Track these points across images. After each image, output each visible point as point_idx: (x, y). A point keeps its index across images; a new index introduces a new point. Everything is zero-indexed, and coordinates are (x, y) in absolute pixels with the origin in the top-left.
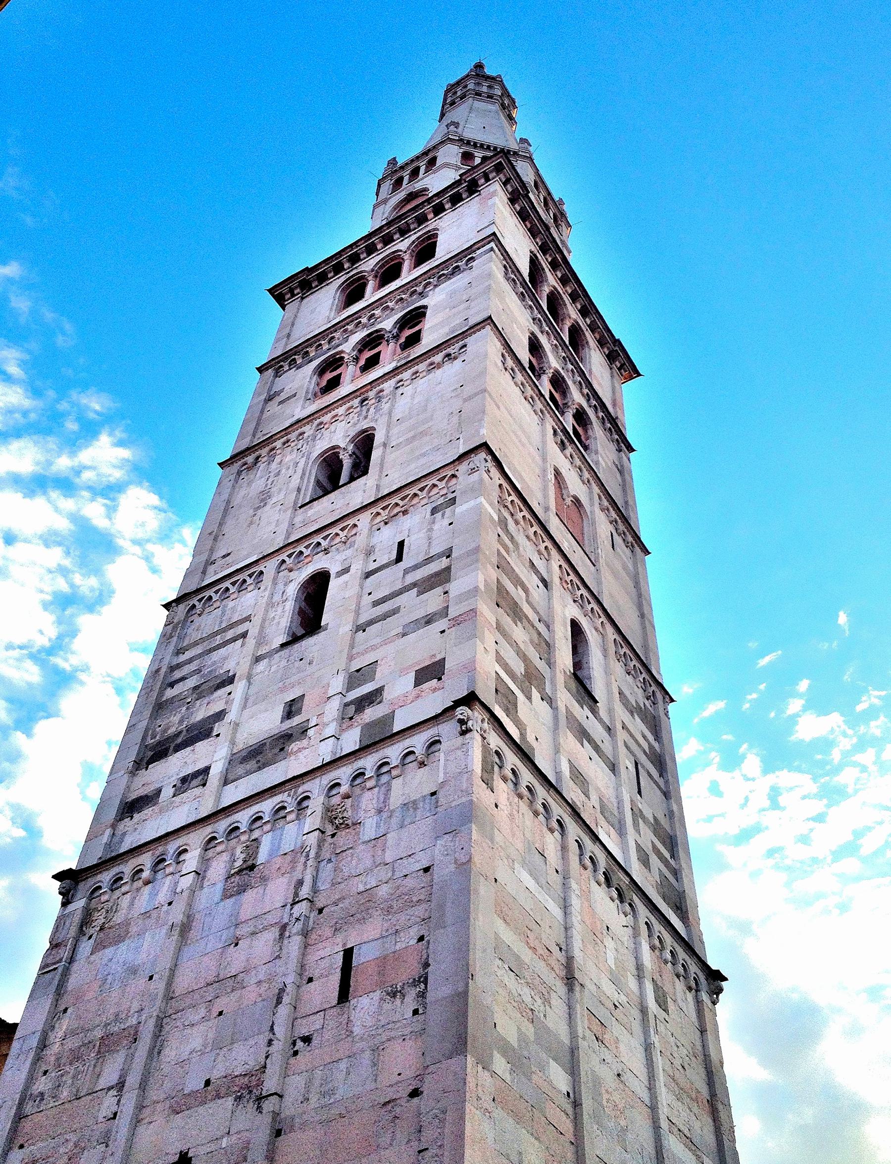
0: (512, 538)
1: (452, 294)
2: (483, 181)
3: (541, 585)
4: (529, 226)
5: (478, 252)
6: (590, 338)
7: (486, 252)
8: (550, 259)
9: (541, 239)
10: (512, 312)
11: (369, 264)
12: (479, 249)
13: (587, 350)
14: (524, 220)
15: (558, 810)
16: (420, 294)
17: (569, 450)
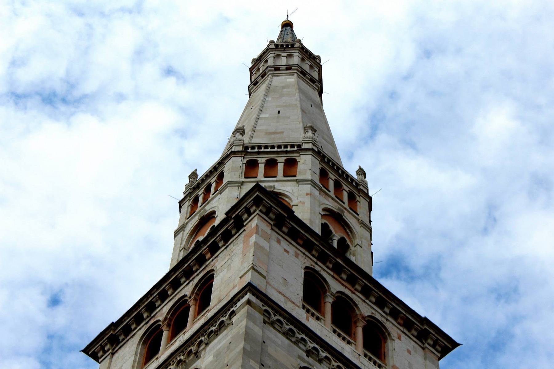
1: (218, 356)
2: (246, 216)
4: (301, 242)
5: (239, 304)
7: (243, 306)
8: (331, 266)
9: (317, 251)
10: (276, 361)
11: (163, 312)
12: (239, 300)
13: (389, 341)
16: (196, 354)
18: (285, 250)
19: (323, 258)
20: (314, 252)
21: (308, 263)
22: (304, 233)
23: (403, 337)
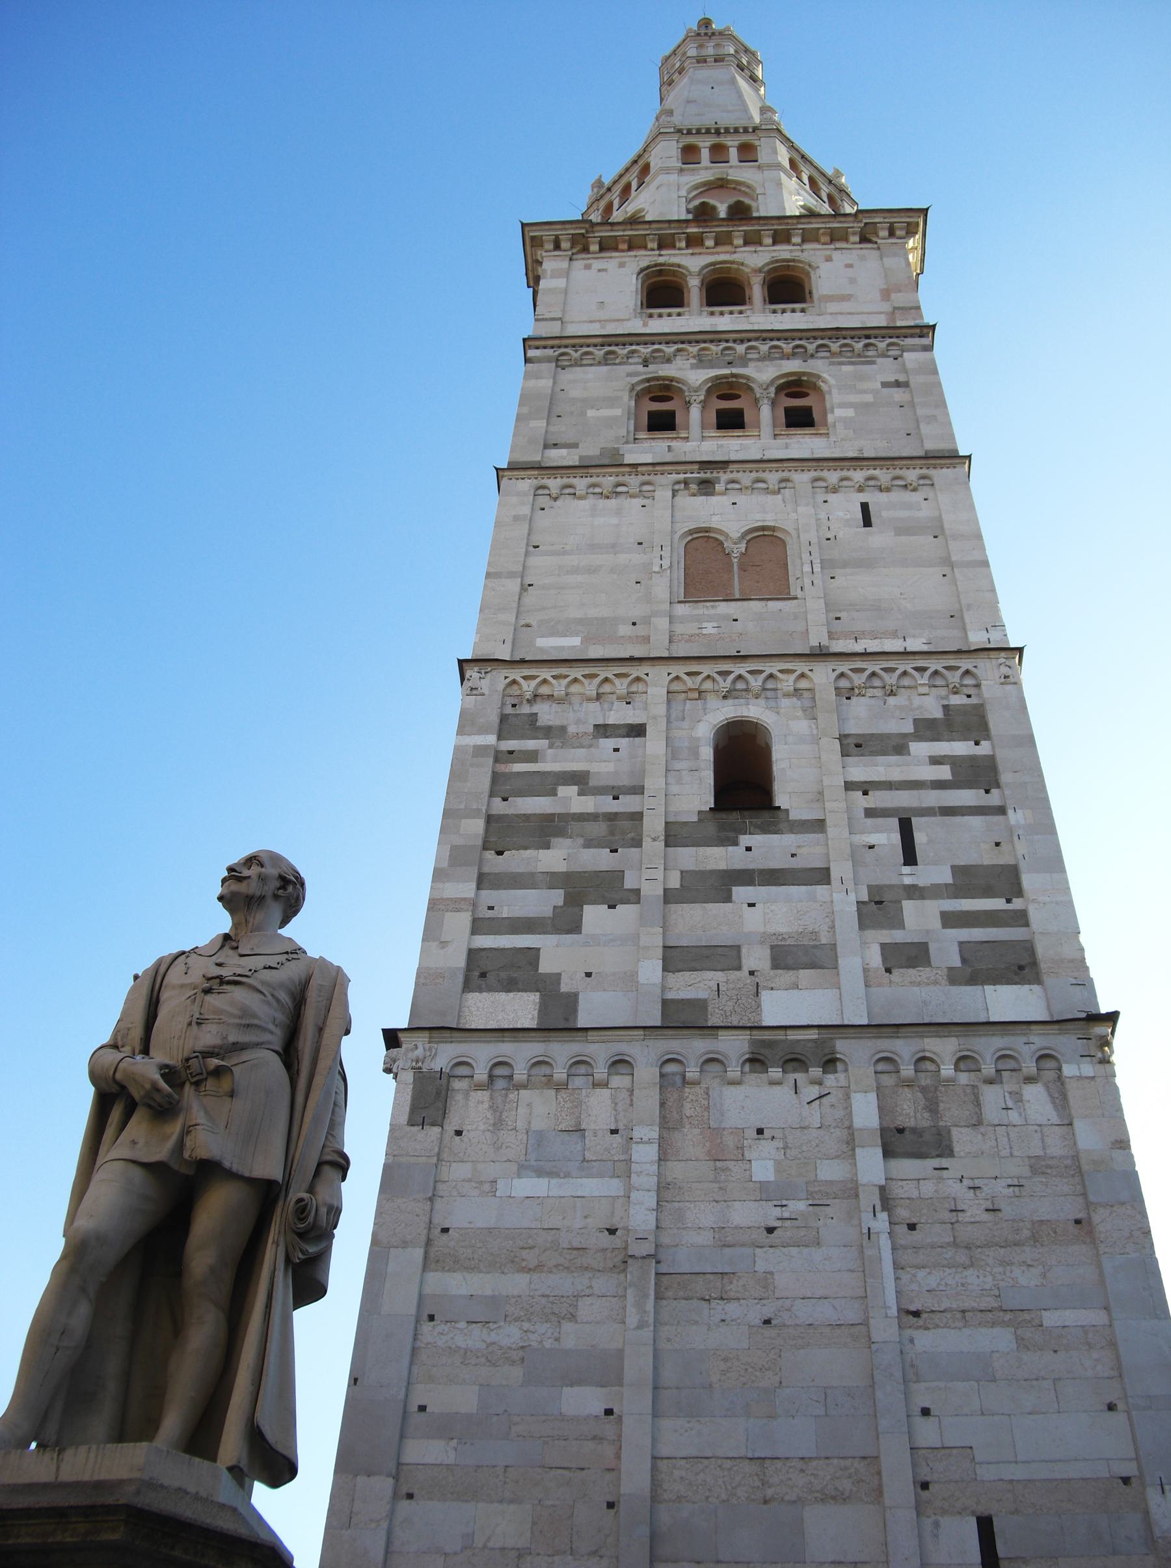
0: (548, 732)
3: (623, 743)
6: (811, 254)
8: (683, 244)
9: (652, 241)
14: (616, 249)
15: (600, 1052)
17: (724, 477)
18: (599, 271)
19: (665, 243)
20: (650, 245)
21: (645, 263)
22: (621, 233)
23: (836, 255)
